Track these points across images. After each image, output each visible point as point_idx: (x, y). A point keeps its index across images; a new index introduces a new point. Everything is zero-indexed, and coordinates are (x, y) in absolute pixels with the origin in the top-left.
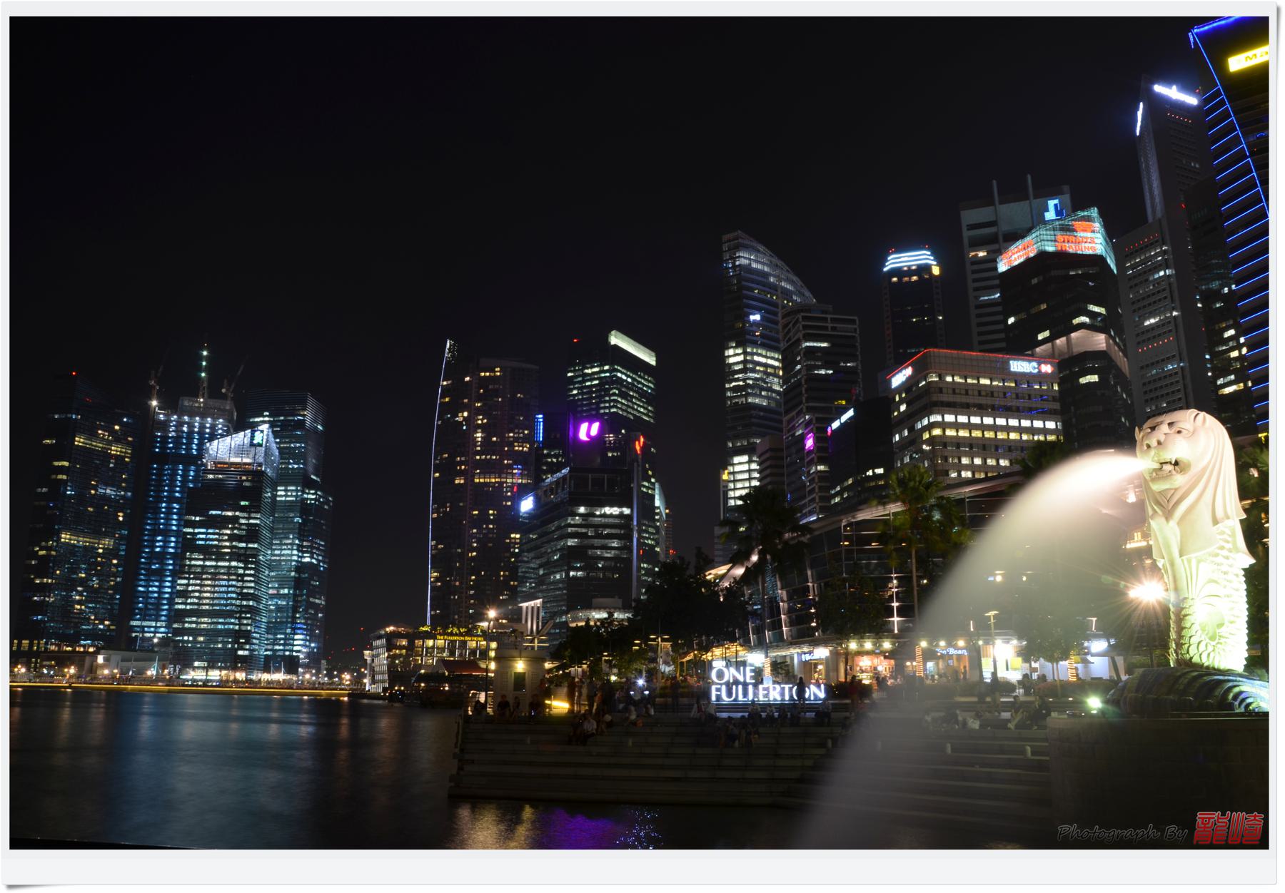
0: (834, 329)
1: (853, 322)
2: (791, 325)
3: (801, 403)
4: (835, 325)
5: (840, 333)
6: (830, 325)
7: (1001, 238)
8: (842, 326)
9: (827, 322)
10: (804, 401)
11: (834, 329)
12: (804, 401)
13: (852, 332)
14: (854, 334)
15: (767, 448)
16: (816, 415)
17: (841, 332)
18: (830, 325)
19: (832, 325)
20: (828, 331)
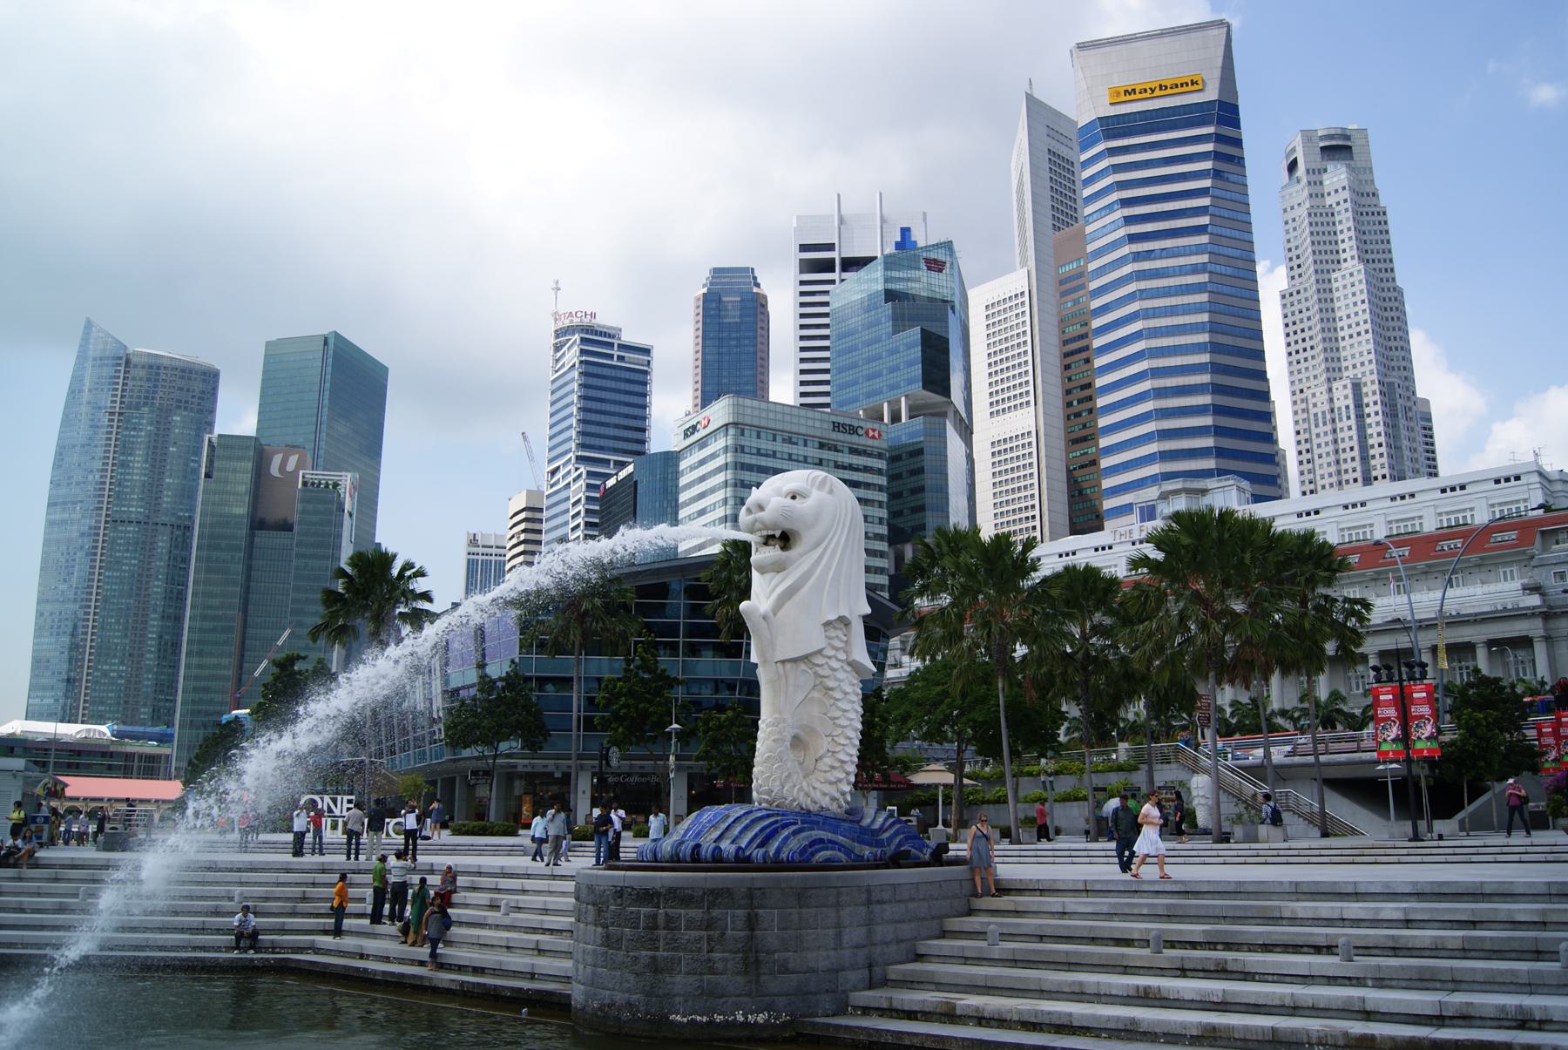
0: (621, 358)
1: (646, 351)
2: (565, 348)
3: (569, 451)
11: (621, 358)
15: (524, 506)
18: (616, 353)
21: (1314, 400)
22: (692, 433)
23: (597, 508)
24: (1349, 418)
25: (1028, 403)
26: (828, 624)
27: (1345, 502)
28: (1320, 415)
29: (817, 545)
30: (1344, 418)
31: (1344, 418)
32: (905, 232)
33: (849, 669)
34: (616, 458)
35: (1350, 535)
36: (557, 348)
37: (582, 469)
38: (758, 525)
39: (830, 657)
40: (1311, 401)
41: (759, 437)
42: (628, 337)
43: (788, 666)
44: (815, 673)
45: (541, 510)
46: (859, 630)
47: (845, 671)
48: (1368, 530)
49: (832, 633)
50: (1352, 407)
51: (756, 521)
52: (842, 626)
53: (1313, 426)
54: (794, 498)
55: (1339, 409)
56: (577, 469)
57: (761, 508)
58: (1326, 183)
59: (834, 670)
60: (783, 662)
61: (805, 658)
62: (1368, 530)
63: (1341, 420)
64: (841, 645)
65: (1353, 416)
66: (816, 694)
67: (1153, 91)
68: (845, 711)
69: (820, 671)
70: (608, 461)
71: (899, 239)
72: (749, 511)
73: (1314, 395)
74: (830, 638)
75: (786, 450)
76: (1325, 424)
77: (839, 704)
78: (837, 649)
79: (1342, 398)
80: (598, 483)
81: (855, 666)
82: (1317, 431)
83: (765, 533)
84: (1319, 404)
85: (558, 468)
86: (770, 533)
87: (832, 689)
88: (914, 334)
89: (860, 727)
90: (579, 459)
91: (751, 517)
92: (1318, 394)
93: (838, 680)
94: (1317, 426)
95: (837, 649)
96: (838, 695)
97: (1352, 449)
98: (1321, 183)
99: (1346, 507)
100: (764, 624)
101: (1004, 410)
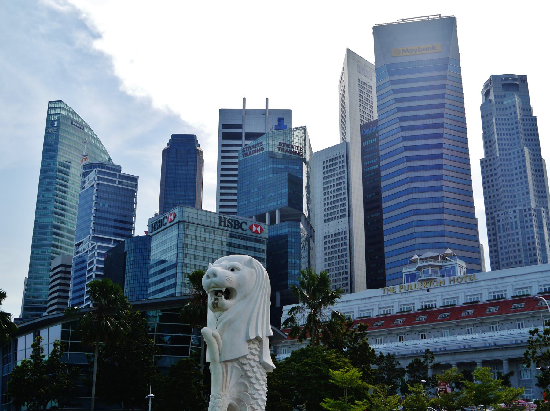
0: (120, 183)
1: (135, 179)
3: (89, 234)
4: (121, 180)
5: (124, 187)
6: (117, 180)
7: (243, 138)
8: (126, 181)
9: (116, 177)
10: (91, 232)
11: (120, 183)
12: (91, 232)
13: (132, 187)
14: (134, 189)
16: (99, 244)
17: (125, 185)
18: (117, 180)
19: (119, 180)
20: (115, 183)
21: (498, 218)
22: (160, 227)
23: (103, 266)
24: (517, 228)
25: (345, 215)
26: (249, 341)
28: (501, 226)
29: (245, 297)
30: (514, 228)
31: (514, 228)
32: (280, 120)
33: (260, 366)
34: (115, 238)
36: (85, 175)
37: (97, 244)
38: (213, 285)
39: (250, 360)
40: (497, 219)
41: (196, 230)
42: (124, 171)
44: (242, 368)
45: (70, 267)
46: (266, 343)
47: (258, 367)
49: (252, 346)
50: (519, 222)
51: (212, 282)
52: (257, 342)
53: (497, 232)
54: (233, 270)
55: (512, 223)
56: (92, 244)
57: (215, 275)
58: (505, 102)
59: (252, 367)
60: (225, 362)
61: (237, 359)
62: (529, 289)
63: (512, 229)
64: (257, 353)
65: (519, 228)
66: (242, 380)
67: (416, 52)
68: (258, 390)
69: (246, 368)
70: (111, 239)
71: (277, 124)
72: (208, 277)
73: (498, 215)
74: (250, 349)
75: (211, 237)
76: (504, 231)
77: (255, 386)
78: (254, 355)
79: (513, 218)
80: (104, 252)
81: (264, 365)
82: (500, 235)
83: (216, 289)
84: (501, 220)
85: (82, 242)
86: (220, 289)
87: (251, 378)
88: (285, 176)
89: (266, 399)
90: (94, 238)
91: (209, 280)
92: (500, 215)
93: (254, 372)
94: (499, 232)
95: (254, 355)
96: (253, 380)
97: (518, 245)
98: (502, 103)
100: (214, 340)
101: (331, 218)
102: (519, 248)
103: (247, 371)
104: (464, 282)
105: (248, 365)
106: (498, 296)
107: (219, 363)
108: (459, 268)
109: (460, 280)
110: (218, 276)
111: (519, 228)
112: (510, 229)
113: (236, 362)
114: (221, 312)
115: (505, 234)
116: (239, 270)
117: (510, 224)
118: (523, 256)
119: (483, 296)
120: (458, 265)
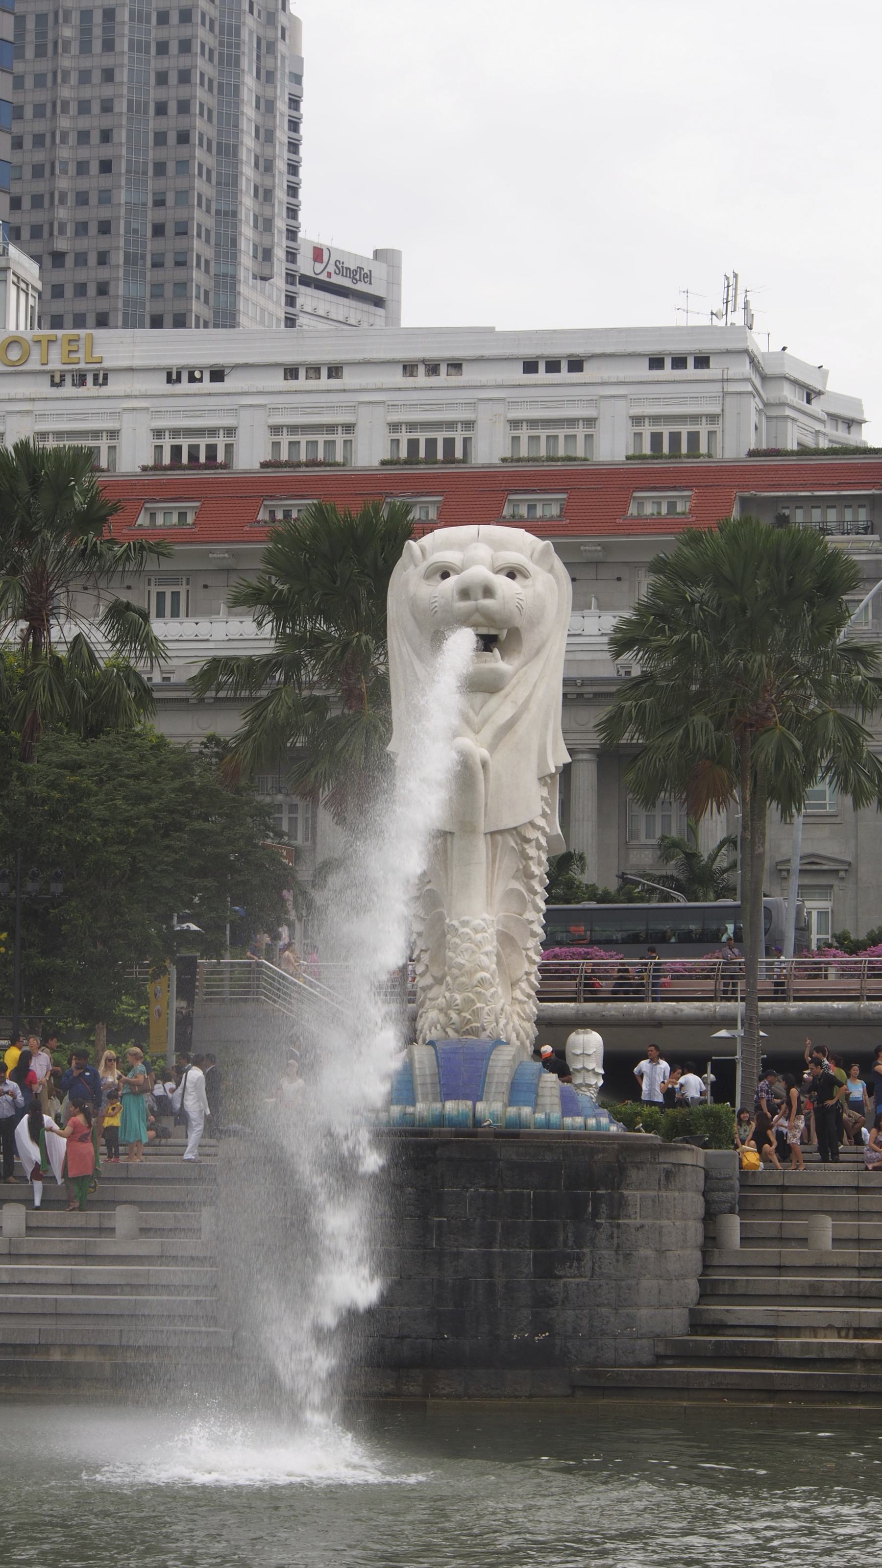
24: (109, 46)
27: (290, 358)
29: (538, 652)
30: (97, 46)
31: (97, 46)
35: (293, 444)
38: (477, 617)
43: (499, 838)
48: (339, 438)
51: (477, 610)
60: (492, 834)
61: (515, 828)
63: (86, 48)
76: (40, 52)
97: (106, 136)
99: (291, 372)
102: (106, 152)
103: (531, 858)
104: (34, 364)
105: (534, 843)
106: (194, 451)
107: (482, 836)
108: (13, 290)
109: (14, 355)
110: (499, 593)
111: (122, 44)
112: (75, 48)
113: (512, 835)
114: (487, 695)
115: (44, 66)
116: (525, 575)
117: (75, 18)
118: (122, 196)
119: (125, 444)
120: (12, 278)
